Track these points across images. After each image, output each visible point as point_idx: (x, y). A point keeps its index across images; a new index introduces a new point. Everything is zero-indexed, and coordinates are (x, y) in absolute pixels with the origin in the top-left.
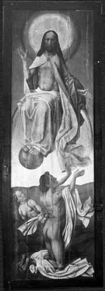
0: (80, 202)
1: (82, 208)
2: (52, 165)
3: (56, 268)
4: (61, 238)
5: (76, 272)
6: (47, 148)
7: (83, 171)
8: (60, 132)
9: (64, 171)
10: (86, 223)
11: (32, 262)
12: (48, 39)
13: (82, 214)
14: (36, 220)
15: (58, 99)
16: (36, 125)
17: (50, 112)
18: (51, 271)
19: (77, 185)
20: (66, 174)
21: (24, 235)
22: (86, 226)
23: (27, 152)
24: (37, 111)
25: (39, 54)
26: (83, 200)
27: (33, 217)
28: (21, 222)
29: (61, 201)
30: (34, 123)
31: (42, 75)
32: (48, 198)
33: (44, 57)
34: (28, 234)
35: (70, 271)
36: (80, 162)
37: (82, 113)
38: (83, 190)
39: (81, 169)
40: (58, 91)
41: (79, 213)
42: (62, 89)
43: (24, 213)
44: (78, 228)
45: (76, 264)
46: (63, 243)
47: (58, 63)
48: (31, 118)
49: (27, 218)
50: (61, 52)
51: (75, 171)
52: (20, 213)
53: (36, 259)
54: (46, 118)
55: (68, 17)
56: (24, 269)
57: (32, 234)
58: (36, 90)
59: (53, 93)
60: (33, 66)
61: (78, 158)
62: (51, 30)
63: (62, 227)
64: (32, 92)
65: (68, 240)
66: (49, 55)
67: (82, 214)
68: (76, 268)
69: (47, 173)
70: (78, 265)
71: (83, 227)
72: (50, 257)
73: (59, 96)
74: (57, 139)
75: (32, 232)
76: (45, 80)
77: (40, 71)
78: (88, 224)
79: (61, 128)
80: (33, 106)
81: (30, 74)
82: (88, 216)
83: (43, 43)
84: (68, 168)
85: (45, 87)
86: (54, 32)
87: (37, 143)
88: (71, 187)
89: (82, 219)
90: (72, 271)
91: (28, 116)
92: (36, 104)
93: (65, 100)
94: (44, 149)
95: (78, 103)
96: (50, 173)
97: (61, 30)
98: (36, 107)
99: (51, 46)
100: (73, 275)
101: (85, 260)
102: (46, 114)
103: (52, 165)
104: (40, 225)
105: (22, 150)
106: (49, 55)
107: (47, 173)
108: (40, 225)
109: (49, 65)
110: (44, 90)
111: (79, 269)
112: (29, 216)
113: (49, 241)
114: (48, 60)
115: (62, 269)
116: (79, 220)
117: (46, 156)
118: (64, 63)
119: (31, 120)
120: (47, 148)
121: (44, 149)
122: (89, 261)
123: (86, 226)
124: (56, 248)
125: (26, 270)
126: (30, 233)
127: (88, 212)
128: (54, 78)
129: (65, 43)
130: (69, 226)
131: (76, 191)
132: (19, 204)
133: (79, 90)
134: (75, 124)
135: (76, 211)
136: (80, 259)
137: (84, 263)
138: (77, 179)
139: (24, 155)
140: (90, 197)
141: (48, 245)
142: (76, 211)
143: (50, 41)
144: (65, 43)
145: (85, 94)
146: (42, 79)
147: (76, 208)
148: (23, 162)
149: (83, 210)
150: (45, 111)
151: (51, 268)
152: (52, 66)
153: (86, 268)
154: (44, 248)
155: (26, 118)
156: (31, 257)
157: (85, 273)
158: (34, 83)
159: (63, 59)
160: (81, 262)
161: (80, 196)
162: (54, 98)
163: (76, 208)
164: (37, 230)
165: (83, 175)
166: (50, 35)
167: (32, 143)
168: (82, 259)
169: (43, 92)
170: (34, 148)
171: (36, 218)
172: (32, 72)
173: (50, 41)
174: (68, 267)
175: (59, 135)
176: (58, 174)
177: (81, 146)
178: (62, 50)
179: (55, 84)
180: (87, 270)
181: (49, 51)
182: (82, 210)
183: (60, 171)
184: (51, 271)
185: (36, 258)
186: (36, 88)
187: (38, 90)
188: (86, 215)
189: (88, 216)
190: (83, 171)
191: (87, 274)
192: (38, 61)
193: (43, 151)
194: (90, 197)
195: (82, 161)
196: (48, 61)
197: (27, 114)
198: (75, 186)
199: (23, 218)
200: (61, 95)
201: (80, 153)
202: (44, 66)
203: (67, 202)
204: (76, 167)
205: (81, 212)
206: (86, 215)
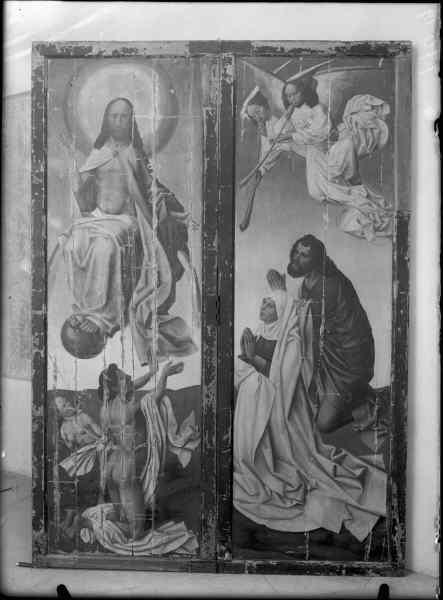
0: (174, 421)
1: (178, 432)
2: (121, 351)
3: (128, 535)
4: (138, 485)
5: (166, 544)
6: (112, 320)
7: (181, 364)
8: (139, 292)
9: (145, 364)
10: (185, 459)
11: (85, 523)
12: (115, 116)
13: (178, 442)
14: (91, 450)
15: (135, 230)
16: (93, 278)
17: (119, 255)
18: (120, 540)
19: (169, 390)
20: (147, 369)
21: (71, 475)
22: (184, 465)
23: (77, 327)
24: (93, 255)
25: (99, 144)
26: (180, 418)
27: (86, 444)
28: (65, 453)
29: (139, 419)
30: (89, 274)
31: (103, 184)
32: (118, 412)
33: (107, 150)
34: (78, 474)
35: (154, 543)
36: (175, 349)
37: (181, 256)
38: (183, 401)
39: (175, 360)
40: (136, 215)
41: (172, 441)
42: (141, 208)
43: (70, 437)
44: (171, 469)
45: (166, 531)
46: (142, 495)
47: (134, 160)
48: (84, 264)
49: (77, 445)
50: (141, 140)
51: (167, 362)
52: (64, 437)
53: (92, 519)
54: (112, 266)
55: (153, 72)
56: (71, 535)
57: (86, 475)
58: (93, 213)
59: (126, 219)
60: (88, 166)
61: (171, 339)
62: (122, 96)
64: (84, 216)
65: (150, 488)
66: (117, 146)
67: (178, 442)
68: (165, 538)
69: (113, 367)
70: (168, 533)
71: (179, 467)
72: (116, 517)
73: (137, 224)
74: (132, 304)
75: (85, 468)
76: (108, 195)
77: (101, 176)
78: (188, 460)
79: (140, 284)
80: (87, 242)
81: (80, 182)
82: (187, 446)
83: (106, 125)
84: (148, 358)
85: (110, 207)
86: (124, 99)
87: (97, 311)
88: (157, 393)
89: (177, 452)
90: (157, 544)
91: (78, 262)
92: (92, 240)
94: (107, 323)
95: (173, 238)
96: (120, 367)
97: (141, 95)
98: (93, 244)
99: (120, 130)
100: (159, 550)
101: (182, 525)
102: (113, 257)
103: (121, 351)
105: (66, 325)
106: (117, 146)
107: (113, 367)
109: (117, 166)
110: (107, 212)
111: (170, 541)
112: (79, 441)
113: (112, 485)
114: (116, 154)
115: (140, 538)
116: (173, 454)
117: (111, 336)
118: (147, 162)
119: (84, 270)
120: (112, 320)
121: (107, 323)
122: (189, 528)
123: (184, 465)
124: (127, 501)
125: (75, 536)
126: (80, 472)
127: (189, 440)
128: (126, 190)
129: (149, 121)
130: (154, 464)
131: (167, 400)
132: (61, 421)
133: (173, 214)
134: (168, 277)
135: (167, 437)
136: (171, 523)
137: (180, 530)
138: (169, 378)
139: (70, 332)
140: (192, 414)
141: (112, 494)
142: (167, 437)
143: (118, 119)
144: (149, 121)
145: (186, 222)
146: (104, 192)
147: (166, 431)
148: (67, 344)
149: (181, 436)
150: (109, 252)
151: (119, 534)
152: (123, 167)
153: (184, 539)
154: (107, 499)
155: (75, 265)
156: (83, 515)
157: (181, 547)
159: (144, 155)
160: (175, 528)
161: (173, 409)
162: (126, 228)
163: (166, 431)
164: (94, 468)
165: (181, 370)
166: (119, 107)
167: (85, 312)
168: (177, 522)
169: (106, 216)
170: (89, 321)
171: (93, 446)
172: (85, 177)
173: (118, 119)
174: (150, 535)
175: (135, 297)
176: (133, 368)
177: (177, 318)
178: (142, 136)
179: (128, 201)
180: (187, 541)
181: (116, 139)
182: (178, 436)
183: (138, 363)
184: (120, 540)
185: (92, 517)
186: (93, 210)
187: (97, 213)
188: (187, 443)
189: (187, 446)
190: (181, 364)
191: (185, 549)
192: (97, 157)
193: (107, 327)
194: (192, 414)
195: (181, 346)
196: (115, 156)
197: (76, 256)
198: (165, 392)
199: (69, 445)
200: (140, 224)
201: (175, 331)
202: (107, 167)
203: (149, 420)
204: (168, 357)
205: (175, 439)
206: (187, 443)
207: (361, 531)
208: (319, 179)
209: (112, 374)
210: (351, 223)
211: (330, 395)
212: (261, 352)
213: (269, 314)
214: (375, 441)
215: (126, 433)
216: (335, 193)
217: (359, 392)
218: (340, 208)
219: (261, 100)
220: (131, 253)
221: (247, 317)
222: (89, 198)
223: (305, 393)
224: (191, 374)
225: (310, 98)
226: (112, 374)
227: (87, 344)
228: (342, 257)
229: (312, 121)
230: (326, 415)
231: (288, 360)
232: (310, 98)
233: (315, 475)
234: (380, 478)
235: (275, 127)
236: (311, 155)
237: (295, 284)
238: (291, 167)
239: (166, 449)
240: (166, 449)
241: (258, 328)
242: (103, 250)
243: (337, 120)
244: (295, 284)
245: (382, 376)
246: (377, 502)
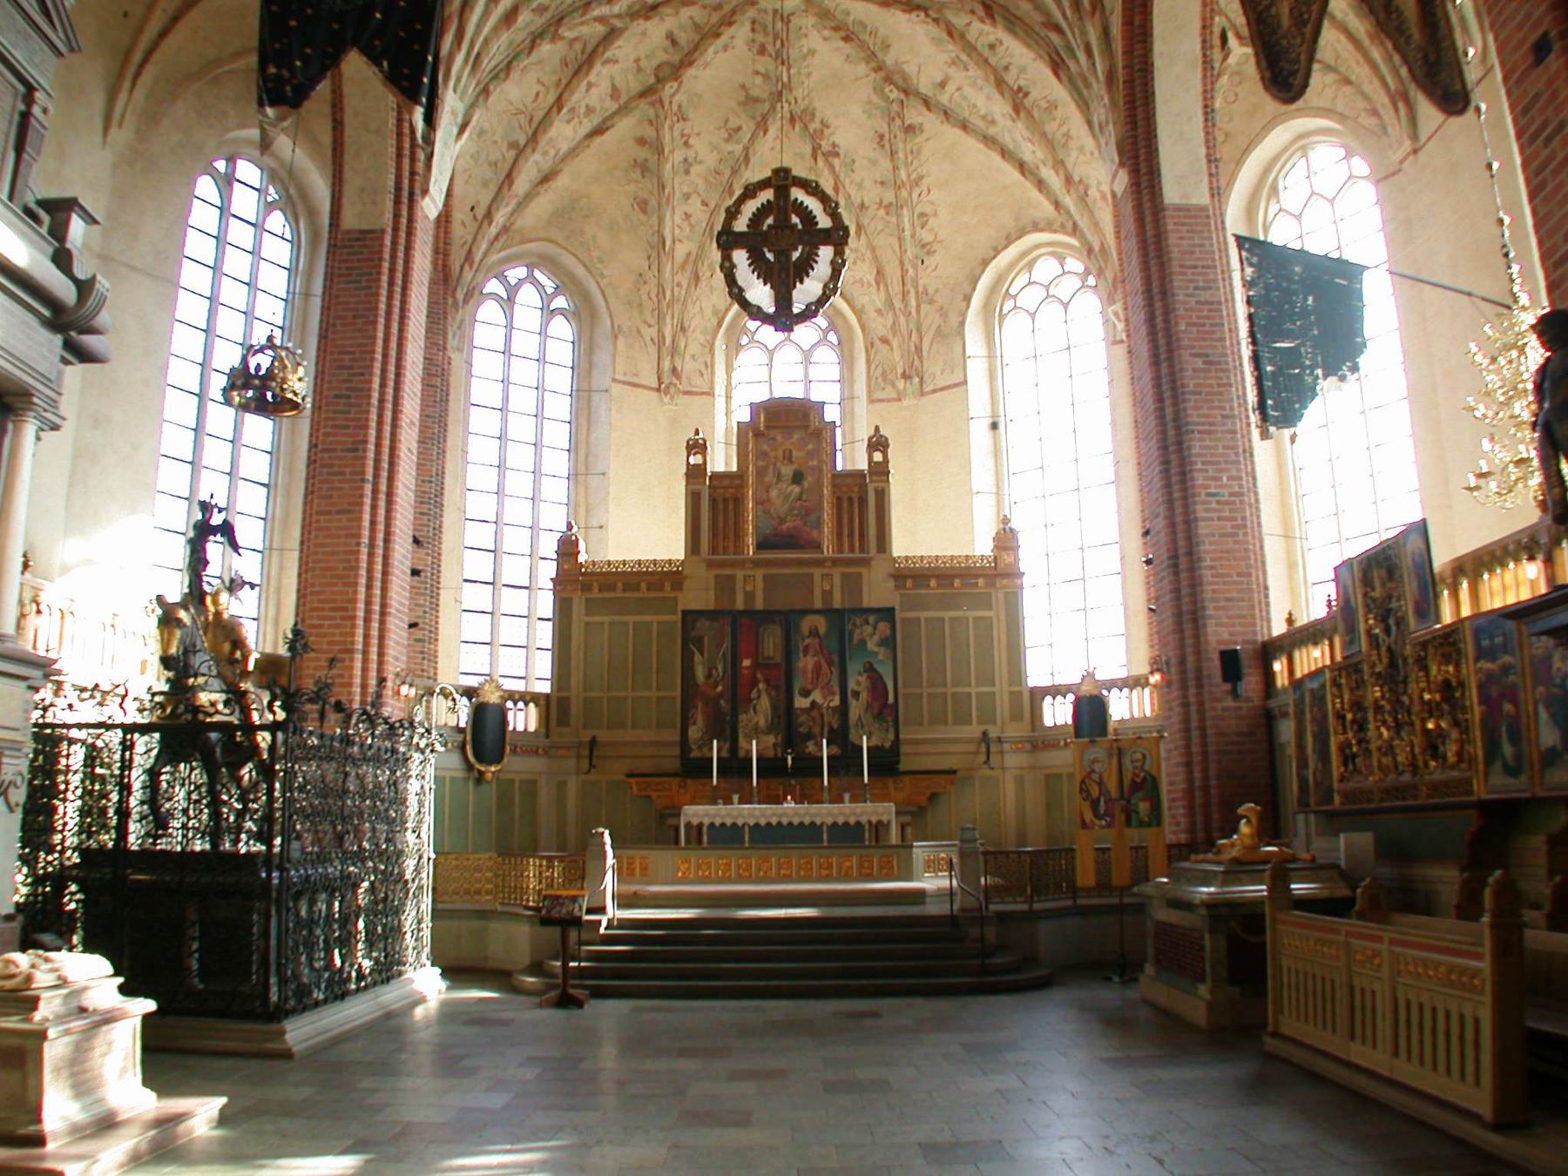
2: (816, 696)
28: (801, 725)
29: (822, 716)
32: (814, 713)
38: (834, 709)
63: (823, 728)
76: (812, 651)
84: (825, 697)
93: (823, 662)
95: (830, 663)
99: (814, 633)
103: (816, 696)
104: (810, 728)
108: (810, 728)
129: (822, 630)
144: (822, 630)
148: (801, 695)
158: (806, 651)
176: (819, 700)
192: (807, 641)
195: (833, 694)
198: (828, 707)
207: (888, 745)
208: (871, 646)
209: (813, 703)
210: (881, 657)
211: (876, 706)
212: (856, 694)
213: (858, 683)
214: (890, 719)
215: (818, 719)
216: (876, 649)
217: (885, 705)
218: (876, 654)
219: (854, 624)
220: (818, 667)
221: (852, 685)
222: (806, 651)
223: (868, 707)
224: (836, 701)
225: (867, 623)
226: (813, 703)
227: (806, 693)
228: (880, 669)
229: (869, 629)
230: (876, 711)
231: (864, 696)
232: (867, 623)
233: (873, 729)
234: (892, 730)
235: (858, 631)
236: (868, 639)
237: (865, 675)
238: (863, 642)
239: (830, 724)
240: (830, 724)
241: (856, 688)
242: (810, 667)
243: (875, 628)
244: (865, 675)
245: (891, 700)
246: (891, 736)
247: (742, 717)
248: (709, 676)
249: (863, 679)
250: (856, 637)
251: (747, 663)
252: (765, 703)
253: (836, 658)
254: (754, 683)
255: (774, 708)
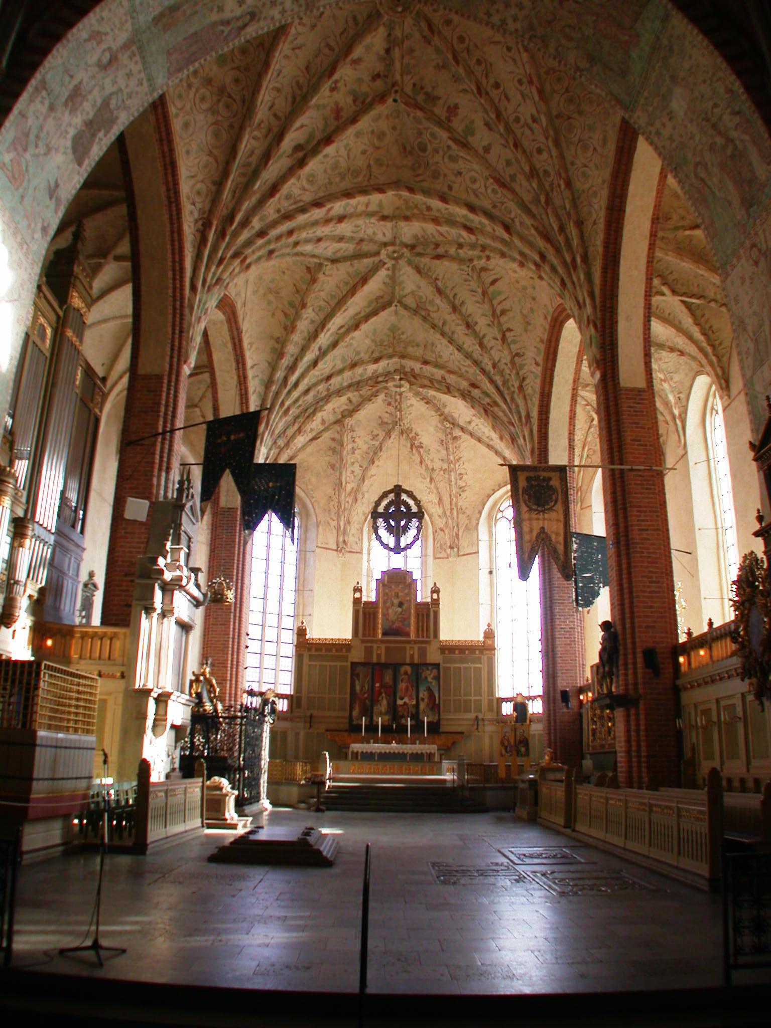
2: (406, 700)
38: (414, 705)
95: (412, 686)
99: (406, 673)
103: (406, 700)
208: (429, 679)
209: (405, 703)
212: (423, 699)
217: (434, 704)
221: (421, 695)
223: (428, 705)
224: (414, 702)
226: (405, 703)
227: (402, 699)
228: (432, 688)
229: (428, 672)
231: (426, 700)
238: (426, 678)
245: (437, 702)
246: (437, 717)
247: (375, 708)
248: (362, 690)
249: (426, 693)
250: (423, 675)
251: (377, 685)
252: (385, 702)
253: (415, 684)
254: (380, 693)
255: (388, 704)
